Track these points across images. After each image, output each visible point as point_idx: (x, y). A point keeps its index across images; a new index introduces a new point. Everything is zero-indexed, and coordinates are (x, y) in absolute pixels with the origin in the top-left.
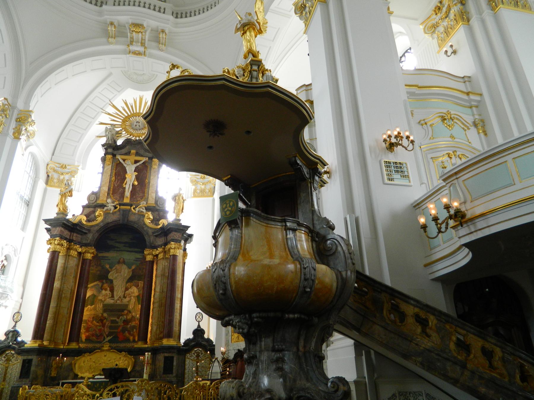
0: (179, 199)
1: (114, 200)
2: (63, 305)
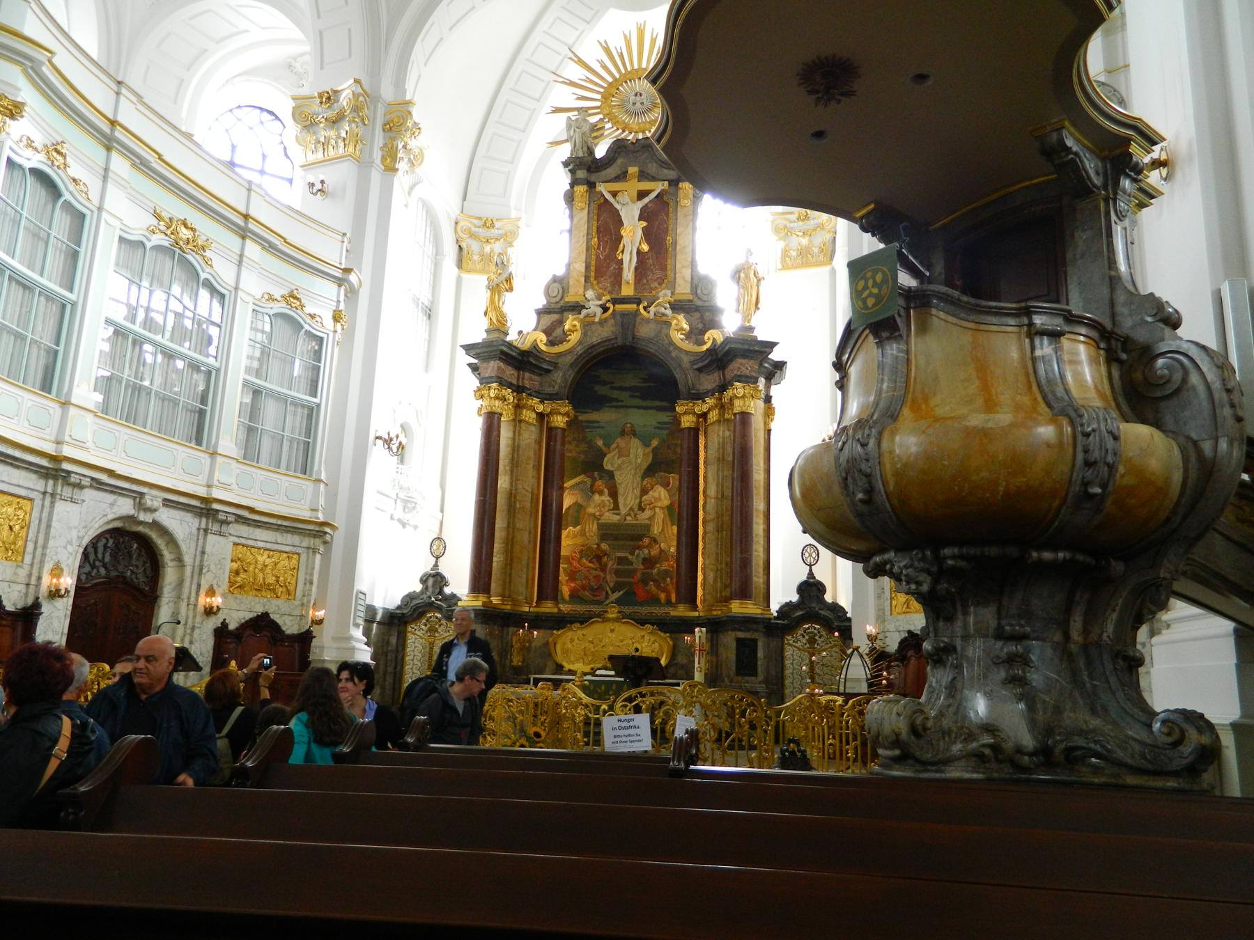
0: (747, 277)
1: (601, 291)
2: (519, 525)
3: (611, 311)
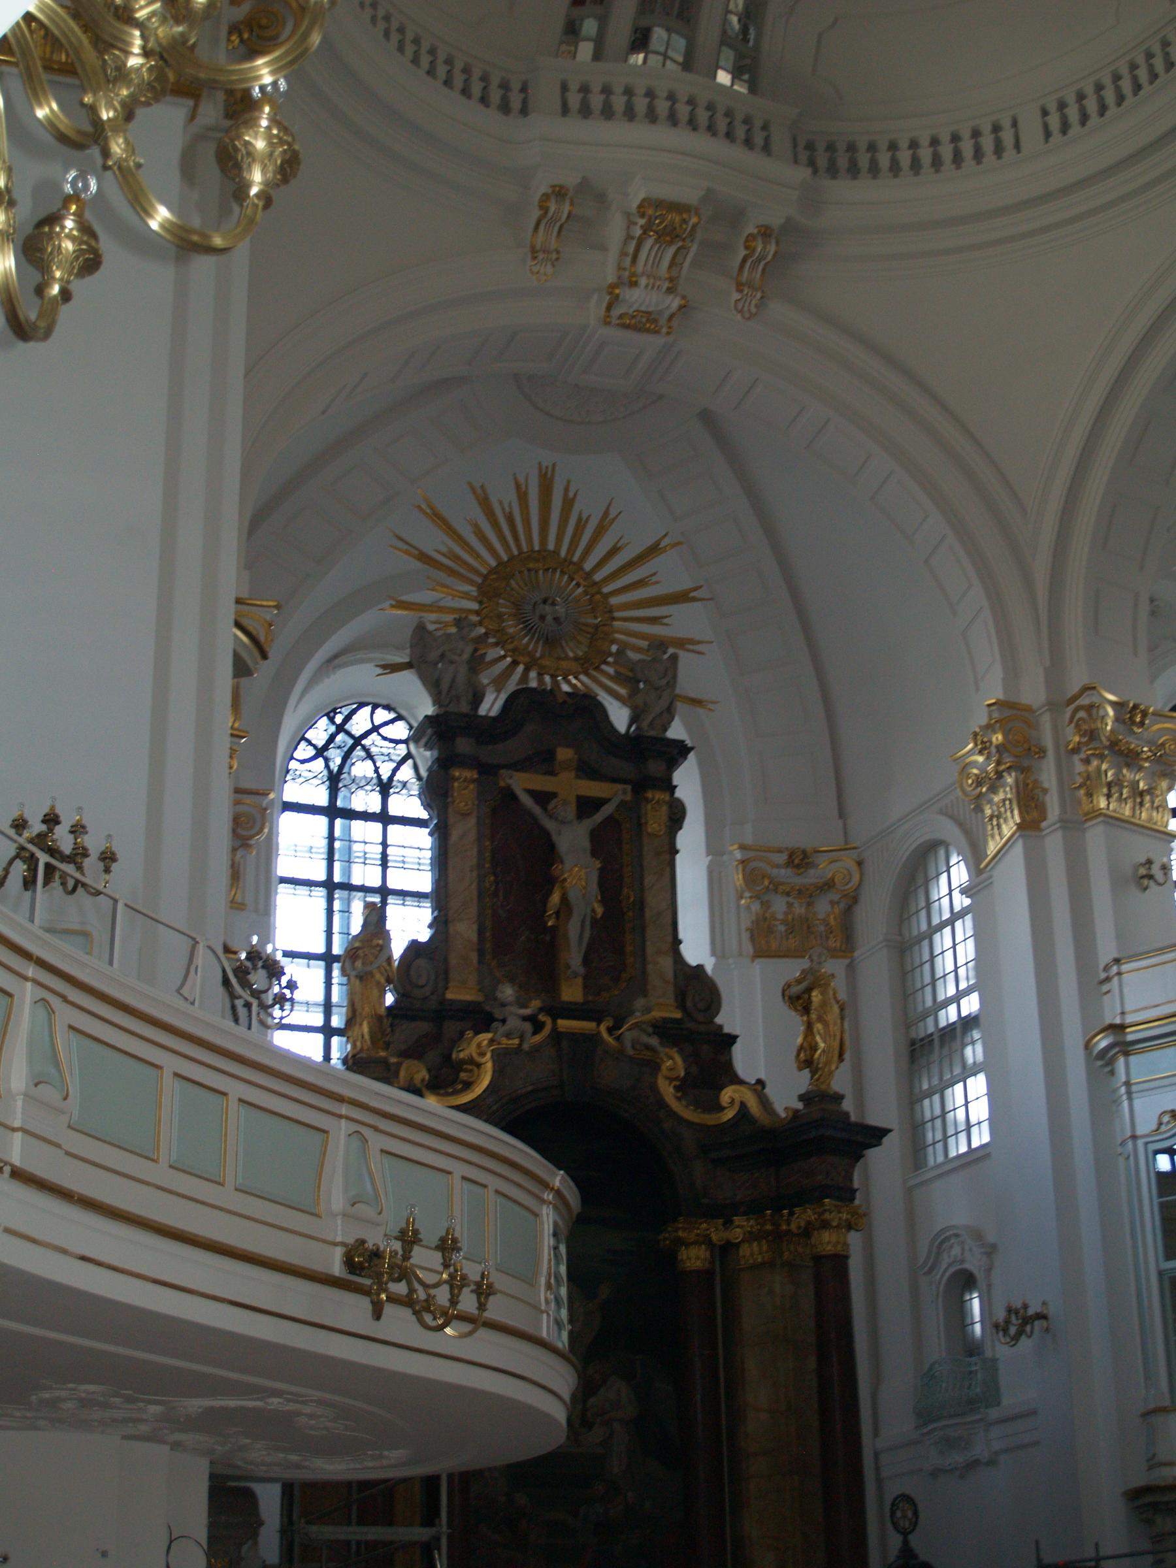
0: (824, 1004)
3: (547, 1031)
